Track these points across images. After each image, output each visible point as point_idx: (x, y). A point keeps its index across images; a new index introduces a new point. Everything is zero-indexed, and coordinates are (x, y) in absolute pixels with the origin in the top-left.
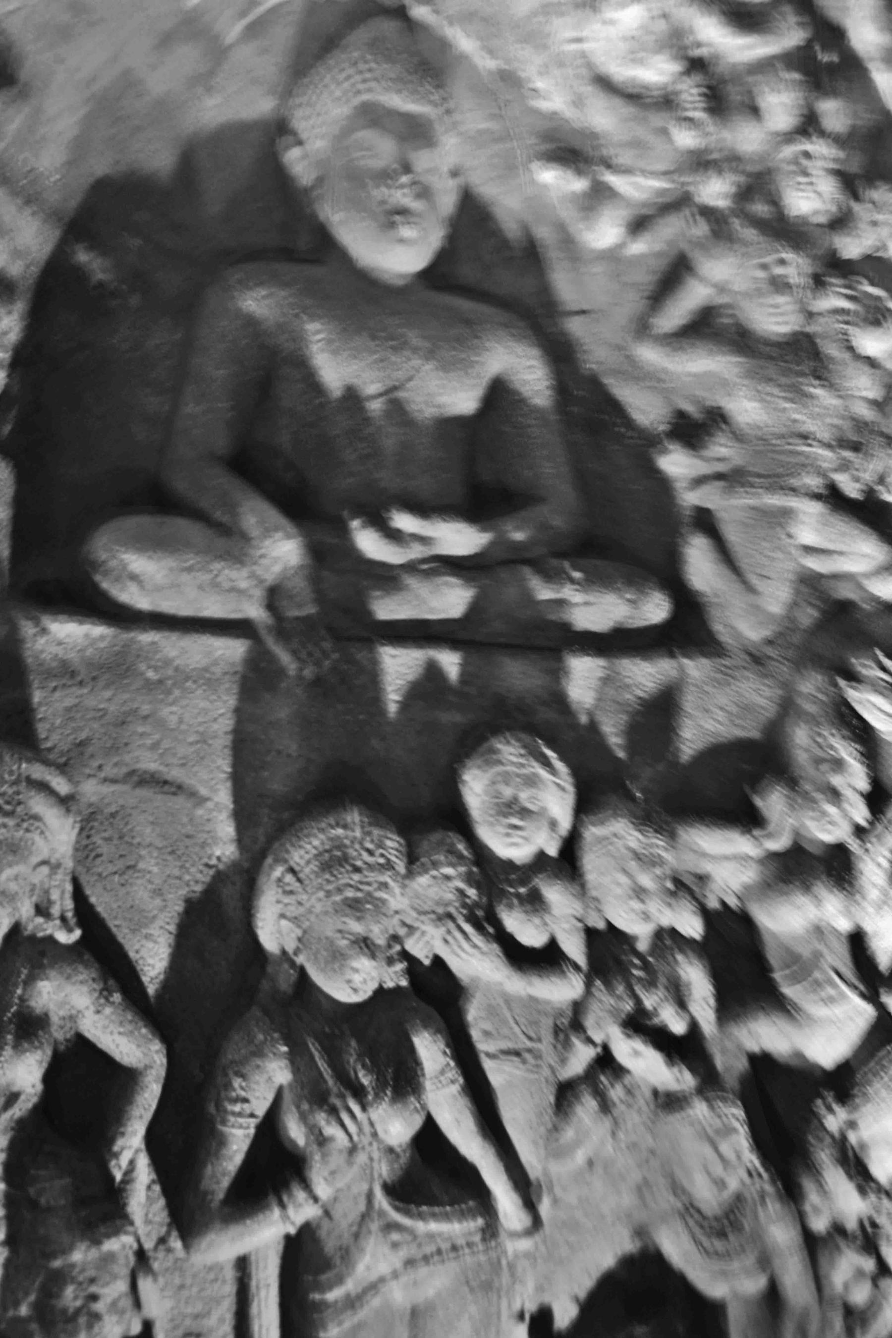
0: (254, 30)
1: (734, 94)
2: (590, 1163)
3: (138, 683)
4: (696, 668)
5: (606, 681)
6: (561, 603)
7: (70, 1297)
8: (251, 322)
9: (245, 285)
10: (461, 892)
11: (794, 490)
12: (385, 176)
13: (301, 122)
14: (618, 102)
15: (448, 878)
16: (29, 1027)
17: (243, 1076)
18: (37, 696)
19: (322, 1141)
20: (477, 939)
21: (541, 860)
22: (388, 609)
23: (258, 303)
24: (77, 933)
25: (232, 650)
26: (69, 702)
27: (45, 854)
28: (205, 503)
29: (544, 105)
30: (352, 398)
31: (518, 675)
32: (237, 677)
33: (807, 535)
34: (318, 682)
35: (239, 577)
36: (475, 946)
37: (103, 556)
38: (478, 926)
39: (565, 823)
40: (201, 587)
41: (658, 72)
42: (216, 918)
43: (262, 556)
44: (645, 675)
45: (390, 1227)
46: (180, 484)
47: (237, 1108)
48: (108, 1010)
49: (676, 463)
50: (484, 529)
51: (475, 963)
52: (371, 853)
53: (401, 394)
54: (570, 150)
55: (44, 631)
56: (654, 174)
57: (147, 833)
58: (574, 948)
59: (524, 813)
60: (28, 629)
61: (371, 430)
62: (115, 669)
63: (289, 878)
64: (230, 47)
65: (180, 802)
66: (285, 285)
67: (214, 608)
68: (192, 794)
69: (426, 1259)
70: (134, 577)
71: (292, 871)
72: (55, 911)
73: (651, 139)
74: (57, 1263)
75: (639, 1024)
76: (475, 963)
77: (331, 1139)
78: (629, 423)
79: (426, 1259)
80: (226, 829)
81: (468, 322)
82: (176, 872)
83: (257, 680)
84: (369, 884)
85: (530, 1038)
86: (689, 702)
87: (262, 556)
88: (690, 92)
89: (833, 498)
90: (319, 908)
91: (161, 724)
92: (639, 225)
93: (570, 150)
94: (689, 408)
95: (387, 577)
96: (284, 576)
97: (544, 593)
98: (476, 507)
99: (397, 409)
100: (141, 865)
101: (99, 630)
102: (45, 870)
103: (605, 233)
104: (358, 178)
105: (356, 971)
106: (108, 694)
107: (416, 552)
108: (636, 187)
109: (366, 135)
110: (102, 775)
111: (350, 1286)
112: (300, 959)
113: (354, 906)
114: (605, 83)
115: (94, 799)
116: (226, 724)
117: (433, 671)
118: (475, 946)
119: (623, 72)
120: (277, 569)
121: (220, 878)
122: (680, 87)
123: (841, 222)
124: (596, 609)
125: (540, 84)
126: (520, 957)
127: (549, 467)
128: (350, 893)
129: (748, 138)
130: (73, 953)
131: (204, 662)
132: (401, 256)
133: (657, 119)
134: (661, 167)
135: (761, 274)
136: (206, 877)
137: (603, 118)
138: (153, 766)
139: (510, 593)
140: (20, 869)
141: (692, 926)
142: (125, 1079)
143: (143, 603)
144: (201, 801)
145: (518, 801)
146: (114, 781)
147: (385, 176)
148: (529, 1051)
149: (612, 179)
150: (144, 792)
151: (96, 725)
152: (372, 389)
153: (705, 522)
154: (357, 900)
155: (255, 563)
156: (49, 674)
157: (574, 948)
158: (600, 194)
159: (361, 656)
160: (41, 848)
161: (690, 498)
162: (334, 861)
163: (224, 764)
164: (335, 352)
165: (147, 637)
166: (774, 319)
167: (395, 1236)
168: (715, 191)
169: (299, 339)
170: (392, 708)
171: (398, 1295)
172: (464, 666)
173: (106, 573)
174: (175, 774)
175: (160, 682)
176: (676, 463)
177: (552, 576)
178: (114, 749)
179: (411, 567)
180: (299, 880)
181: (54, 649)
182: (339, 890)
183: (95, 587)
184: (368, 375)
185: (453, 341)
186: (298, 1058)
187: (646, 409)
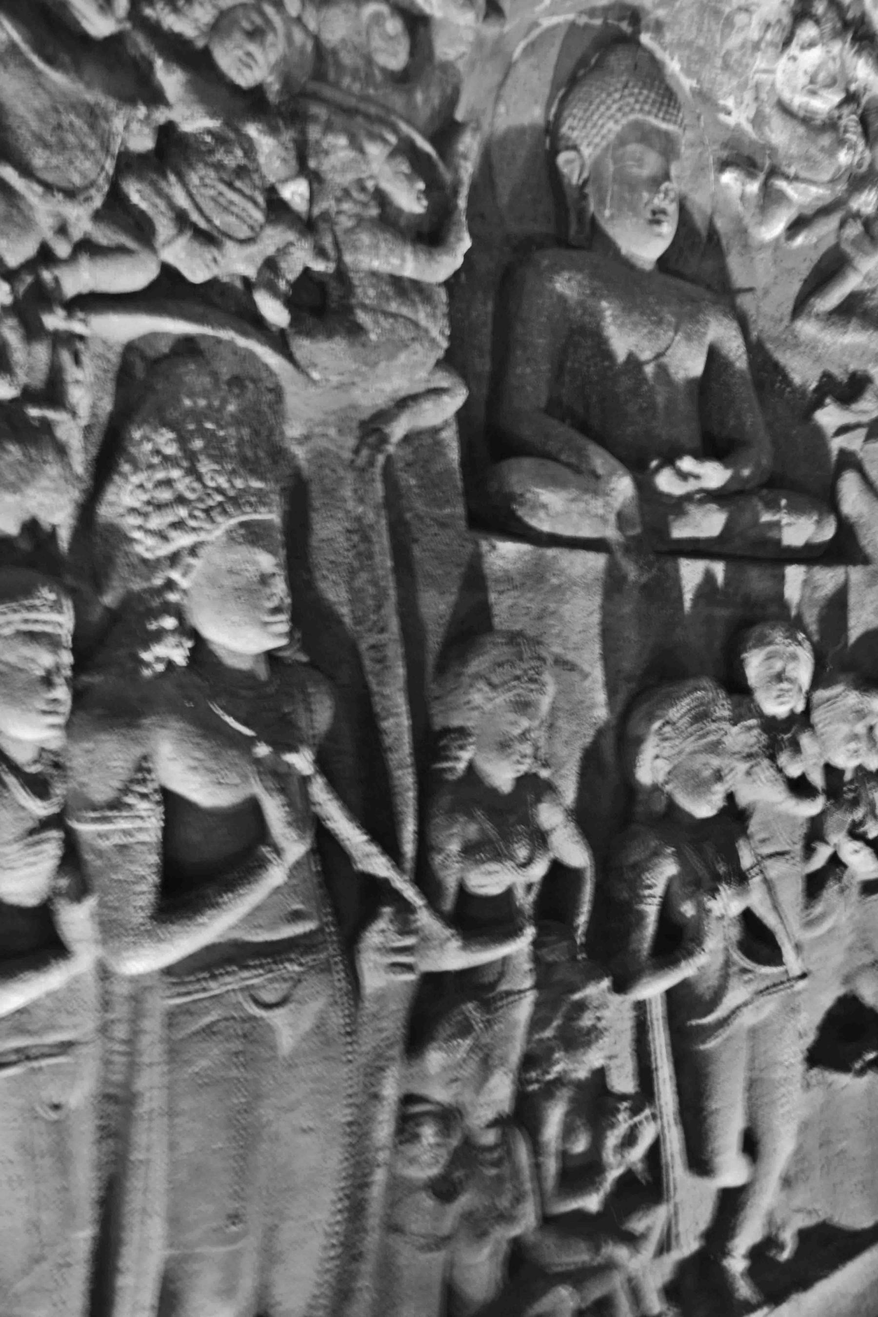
0: (531, 49)
4: (856, 574)
5: (805, 583)
6: (777, 525)
7: (587, 1021)
8: (562, 299)
9: (556, 269)
13: (570, 129)
14: (791, 124)
18: (493, 597)
21: (792, 717)
22: (680, 531)
23: (566, 285)
25: (597, 561)
26: (510, 602)
28: (552, 446)
29: (731, 121)
30: (634, 363)
31: (757, 581)
32: (600, 583)
34: (644, 588)
35: (597, 505)
37: (518, 490)
42: (608, 762)
43: (613, 489)
44: (828, 579)
45: (744, 971)
46: (527, 432)
50: (727, 466)
53: (665, 360)
54: (743, 158)
55: (494, 547)
58: (817, 779)
60: (485, 546)
61: (645, 388)
62: (534, 577)
64: (516, 62)
66: (580, 270)
67: (586, 531)
68: (582, 671)
70: (544, 506)
73: (820, 156)
74: (577, 996)
75: (855, 833)
78: (786, 380)
80: (601, 697)
81: (693, 301)
83: (613, 584)
86: (853, 598)
87: (613, 489)
88: (850, 120)
91: (561, 618)
93: (743, 158)
94: (836, 371)
95: (677, 506)
96: (624, 505)
97: (766, 517)
98: (713, 449)
99: (662, 371)
101: (525, 547)
103: (773, 229)
104: (632, 185)
106: (530, 595)
107: (691, 486)
108: (801, 195)
109: (634, 148)
111: (719, 1013)
112: (668, 788)
114: (784, 109)
116: (596, 618)
117: (709, 577)
120: (621, 499)
121: (600, 733)
124: (799, 530)
125: (730, 103)
127: (752, 419)
132: (645, 246)
133: (826, 140)
136: (592, 732)
137: (780, 135)
139: (747, 516)
142: (576, 875)
143: (545, 527)
144: (586, 676)
145: (778, 673)
149: (781, 184)
151: (526, 619)
152: (646, 355)
153: (849, 461)
155: (608, 495)
156: (497, 581)
159: (669, 565)
161: (836, 444)
162: (701, 716)
163: (596, 649)
164: (621, 326)
165: (551, 552)
167: (746, 977)
169: (597, 315)
170: (687, 604)
171: (747, 1019)
172: (726, 571)
173: (522, 504)
175: (560, 586)
177: (772, 505)
179: (688, 498)
181: (500, 562)
183: (513, 513)
184: (646, 343)
185: (689, 317)
186: (680, 857)
187: (803, 373)
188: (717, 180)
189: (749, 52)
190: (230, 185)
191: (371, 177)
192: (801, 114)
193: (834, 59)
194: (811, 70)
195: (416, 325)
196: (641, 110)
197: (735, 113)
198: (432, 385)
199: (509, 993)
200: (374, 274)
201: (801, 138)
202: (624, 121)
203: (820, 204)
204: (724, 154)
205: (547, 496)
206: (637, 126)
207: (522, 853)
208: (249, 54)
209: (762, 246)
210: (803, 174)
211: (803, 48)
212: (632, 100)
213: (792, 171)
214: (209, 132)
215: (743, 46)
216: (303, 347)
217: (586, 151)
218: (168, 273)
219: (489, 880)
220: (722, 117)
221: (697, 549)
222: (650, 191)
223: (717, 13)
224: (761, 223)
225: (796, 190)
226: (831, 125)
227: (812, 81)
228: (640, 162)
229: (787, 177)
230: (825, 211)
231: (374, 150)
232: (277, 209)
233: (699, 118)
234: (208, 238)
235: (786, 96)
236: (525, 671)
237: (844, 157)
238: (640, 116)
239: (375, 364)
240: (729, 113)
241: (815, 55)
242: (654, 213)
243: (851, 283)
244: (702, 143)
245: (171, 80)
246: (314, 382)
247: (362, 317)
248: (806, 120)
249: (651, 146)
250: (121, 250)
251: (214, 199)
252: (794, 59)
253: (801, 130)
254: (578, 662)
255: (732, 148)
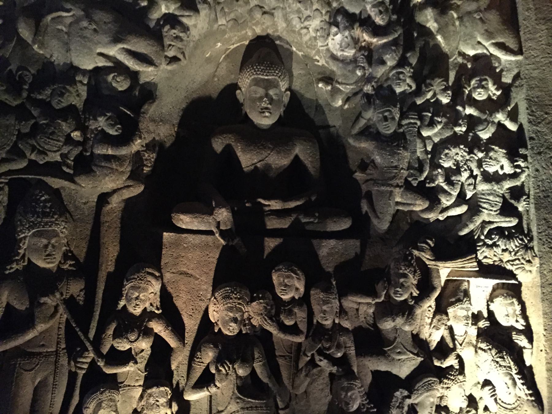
1: (375, 57)
2: (306, 392)
3: (182, 247)
10: (265, 307)
11: (391, 185)
12: (261, 99)
15: (261, 303)
16: (147, 332)
17: (200, 352)
19: (219, 371)
20: (269, 321)
24: (160, 311)
27: (153, 291)
29: (320, 64)
33: (398, 199)
35: (210, 219)
36: (268, 323)
38: (271, 318)
39: (302, 290)
40: (199, 222)
41: (350, 53)
47: (198, 360)
48: (167, 331)
49: (359, 176)
51: (272, 329)
52: (236, 294)
56: (351, 84)
57: (182, 287)
58: (303, 327)
59: (286, 286)
62: (176, 244)
63: (215, 300)
65: (191, 279)
67: (203, 228)
69: (247, 408)
70: (181, 220)
71: (215, 298)
72: (155, 305)
73: (348, 74)
76: (272, 329)
77: (221, 370)
79: (247, 408)
82: (190, 298)
84: (235, 303)
85: (288, 353)
88: (361, 58)
89: (408, 186)
90: (222, 309)
92: (347, 100)
100: (181, 295)
102: (152, 294)
105: (231, 326)
110: (171, 271)
113: (230, 309)
114: (334, 57)
115: (169, 278)
118: (268, 323)
119: (339, 54)
122: (357, 55)
123: (418, 92)
126: (283, 328)
128: (229, 305)
129: (380, 72)
130: (159, 317)
131: (199, 242)
133: (350, 67)
134: (352, 82)
135: (381, 115)
138: (185, 270)
140: (145, 294)
141: (346, 324)
143: (184, 227)
146: (174, 273)
147: (261, 99)
148: (288, 356)
150: (182, 276)
151: (170, 258)
154: (231, 307)
157: (303, 327)
158: (335, 92)
160: (151, 290)
165: (184, 235)
166: (388, 129)
168: (368, 89)
174: (190, 272)
175: (187, 247)
176: (359, 176)
178: (176, 265)
180: (217, 301)
182: (226, 304)
188: (318, 86)
189: (314, 41)
190: (49, 138)
191: (100, 127)
192: (341, 58)
193: (347, 37)
194: (339, 43)
195: (112, 169)
196: (256, 74)
197: (320, 61)
198: (126, 185)
199: (129, 386)
200: (99, 154)
201: (341, 68)
202: (250, 79)
203: (354, 91)
204: (320, 76)
205: (182, 217)
206: (255, 79)
207: (133, 338)
208: (59, 100)
209: (337, 109)
210: (344, 81)
211: (334, 36)
212: (253, 71)
213: (340, 80)
214: (44, 124)
215: (310, 39)
216: (77, 179)
217: (243, 90)
218: (32, 163)
219: (123, 346)
220: (316, 63)
221: (275, 233)
222: (259, 102)
223: (294, 32)
224: (332, 102)
225: (342, 87)
226: (354, 61)
227: (341, 47)
228: (255, 92)
229: (339, 83)
230: (355, 94)
231: (100, 119)
232: (69, 140)
233: (307, 65)
234: (43, 153)
235: (335, 53)
236: (138, 277)
237: (359, 73)
238: (256, 76)
239: (101, 181)
240: (318, 61)
241: (339, 37)
242: (262, 109)
243: (362, 123)
244: (310, 74)
245: (35, 113)
246: (83, 187)
247: (94, 168)
248: (343, 61)
249: (260, 86)
250: (14, 160)
251: (44, 142)
252: (333, 39)
253: (341, 65)
254: (194, 274)
255: (322, 74)
